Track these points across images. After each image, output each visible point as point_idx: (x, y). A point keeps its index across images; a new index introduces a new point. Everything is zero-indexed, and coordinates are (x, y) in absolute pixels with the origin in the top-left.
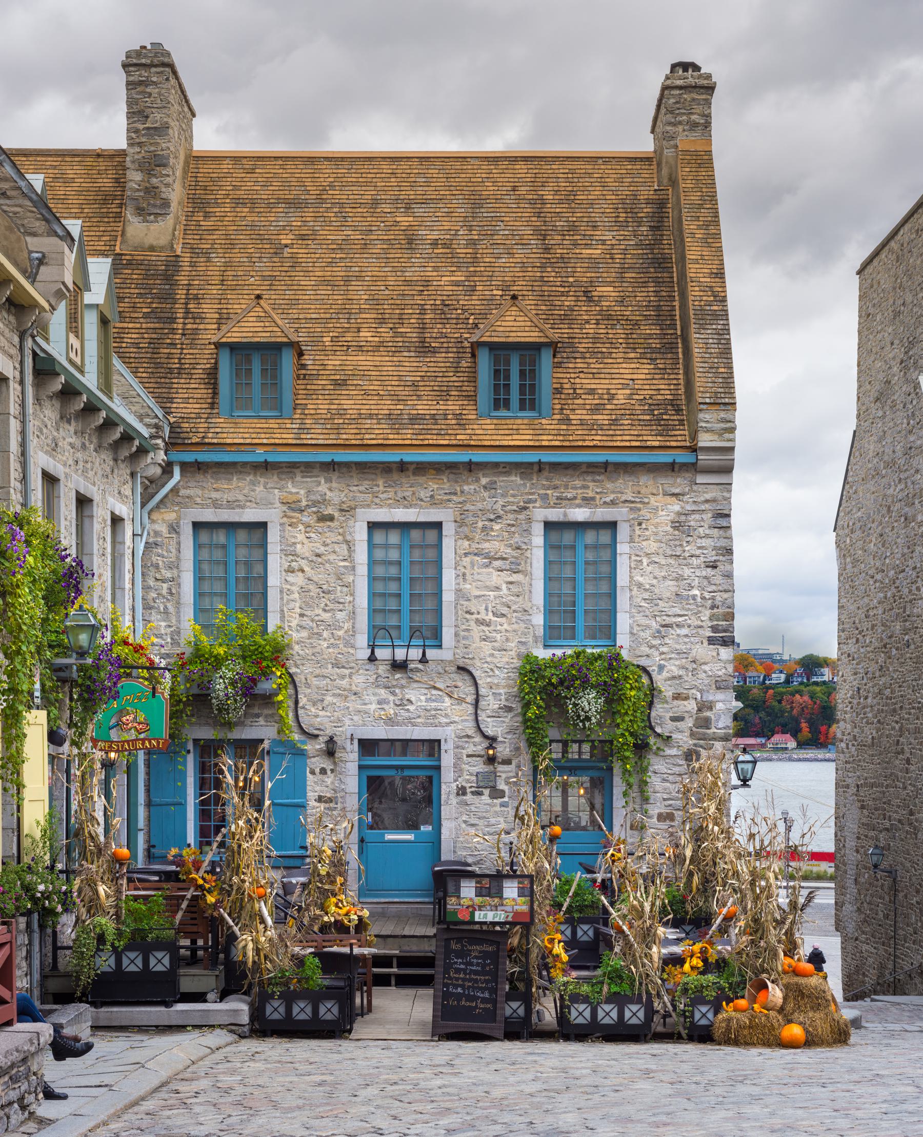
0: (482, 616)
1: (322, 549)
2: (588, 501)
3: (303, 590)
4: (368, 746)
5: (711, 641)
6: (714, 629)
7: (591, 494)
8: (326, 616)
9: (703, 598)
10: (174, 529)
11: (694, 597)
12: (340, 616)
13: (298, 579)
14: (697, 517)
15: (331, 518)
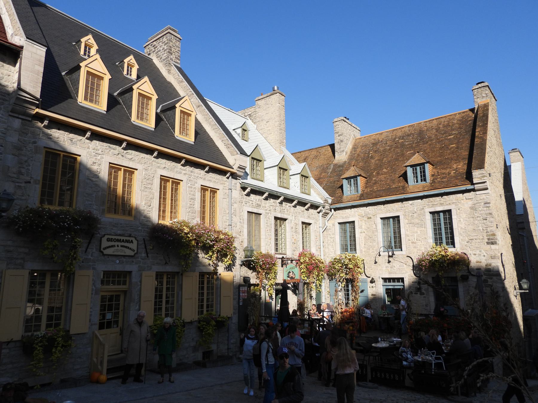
0: (413, 241)
1: (369, 226)
2: (442, 204)
3: (365, 238)
4: (385, 280)
5: (488, 243)
6: (488, 239)
7: (442, 202)
8: (371, 244)
9: (483, 230)
10: (334, 225)
11: (480, 230)
12: (374, 244)
13: (364, 235)
14: (478, 205)
15: (371, 218)
